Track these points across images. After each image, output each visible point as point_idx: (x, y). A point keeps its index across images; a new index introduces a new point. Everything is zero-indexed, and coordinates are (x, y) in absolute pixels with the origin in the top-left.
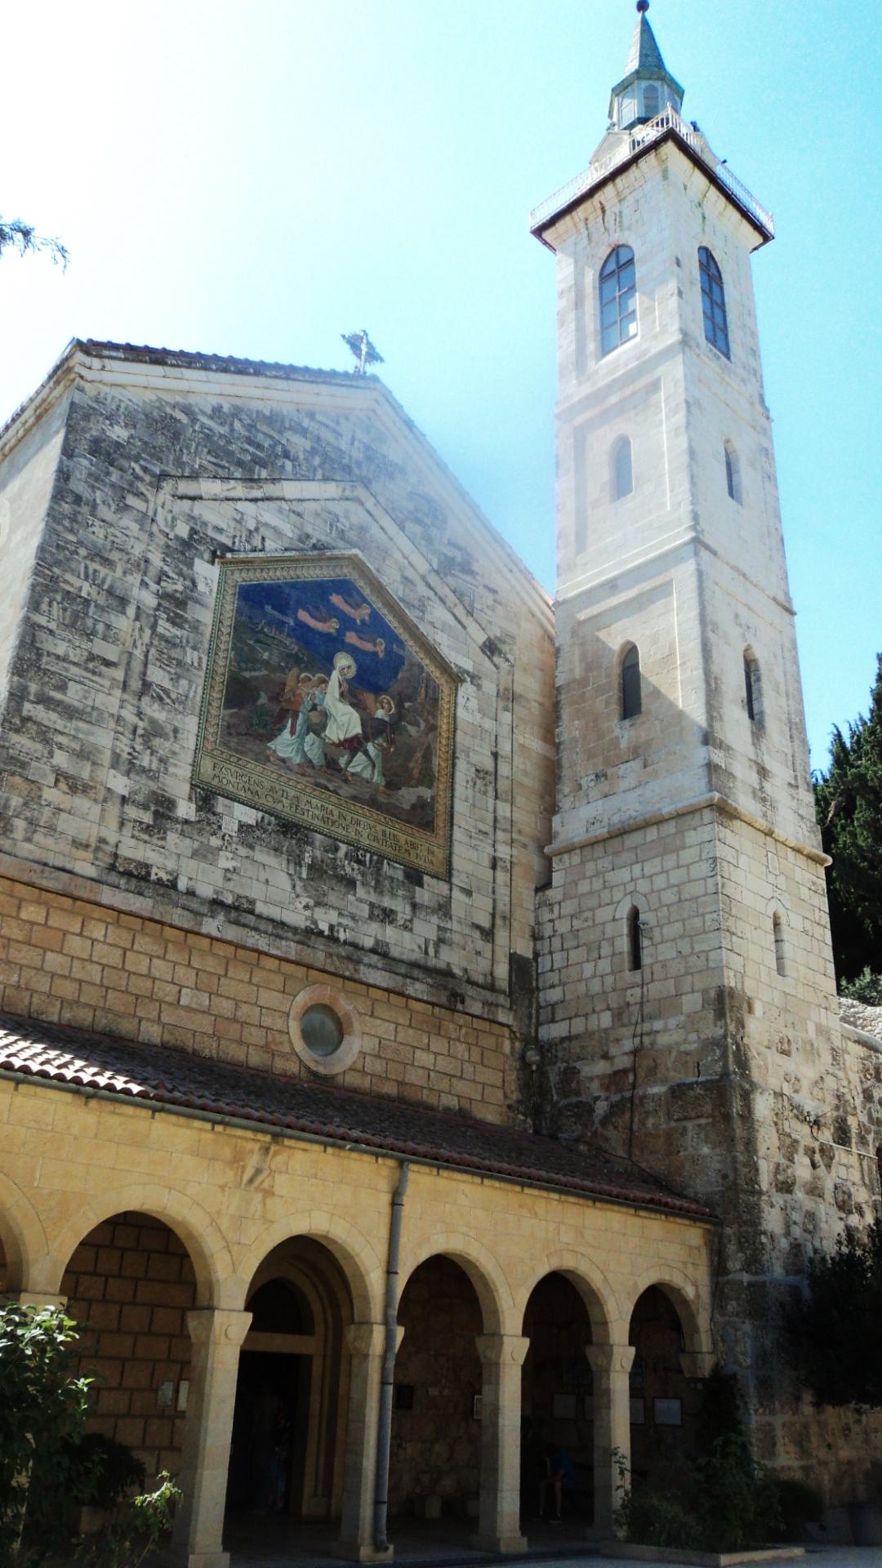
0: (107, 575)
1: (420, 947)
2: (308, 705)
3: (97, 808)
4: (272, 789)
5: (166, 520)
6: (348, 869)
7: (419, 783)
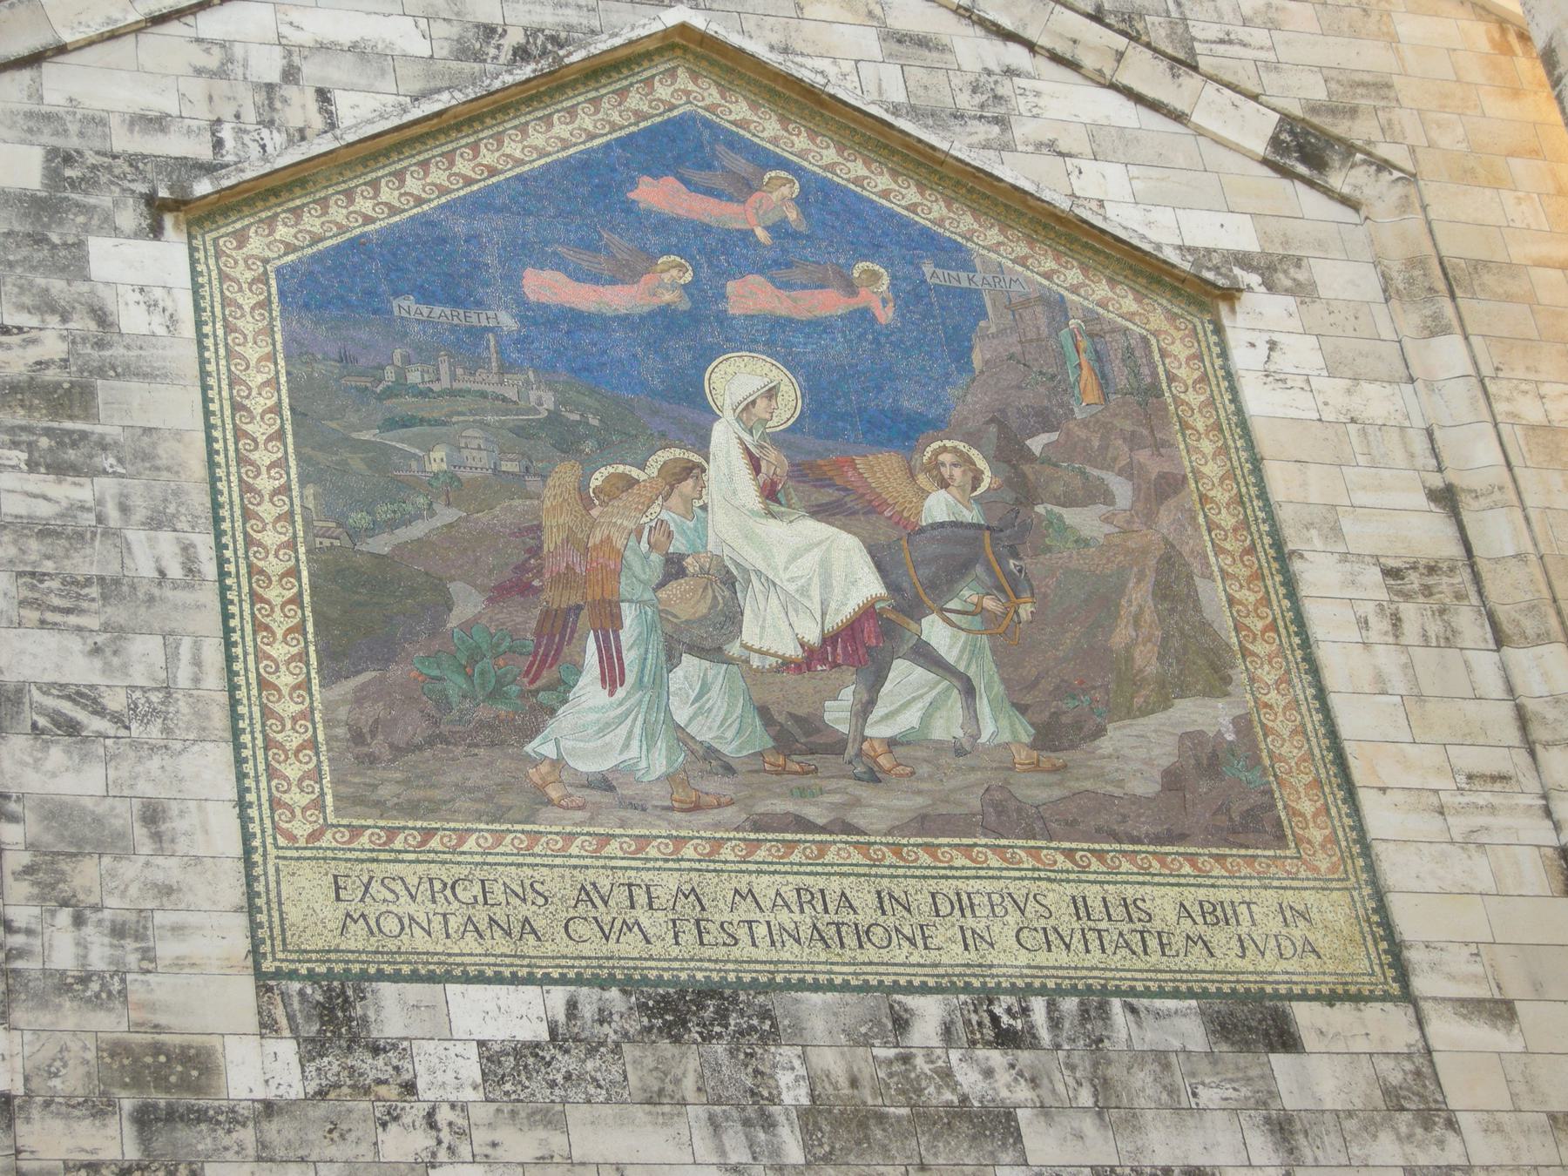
2: (642, 565)
4: (585, 894)
6: (969, 1079)
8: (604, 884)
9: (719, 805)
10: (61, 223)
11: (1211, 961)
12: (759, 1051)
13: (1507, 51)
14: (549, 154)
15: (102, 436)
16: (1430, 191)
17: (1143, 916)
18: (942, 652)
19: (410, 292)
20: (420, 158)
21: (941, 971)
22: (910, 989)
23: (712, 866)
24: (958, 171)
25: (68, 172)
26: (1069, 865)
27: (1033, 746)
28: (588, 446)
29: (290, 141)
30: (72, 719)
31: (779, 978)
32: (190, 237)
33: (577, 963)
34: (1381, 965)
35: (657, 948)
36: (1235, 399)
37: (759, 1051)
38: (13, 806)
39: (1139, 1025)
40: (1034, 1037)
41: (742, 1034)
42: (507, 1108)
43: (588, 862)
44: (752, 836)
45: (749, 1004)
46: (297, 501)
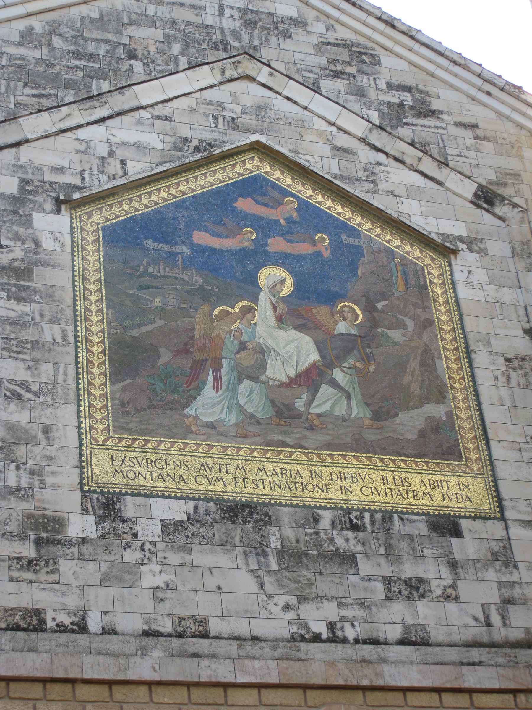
1: (476, 619)
6: (340, 542)
8: (210, 463)
9: (254, 436)
10: (24, 207)
11: (432, 502)
12: (264, 528)
14: (205, 188)
15: (35, 288)
17: (408, 484)
18: (340, 382)
21: (332, 501)
23: (250, 459)
25: (27, 188)
26: (382, 464)
27: (371, 419)
28: (214, 299)
29: (110, 180)
30: (19, 393)
31: (272, 501)
32: (71, 214)
33: (198, 492)
34: (494, 506)
35: (228, 489)
36: (455, 292)
37: (264, 528)
39: (403, 524)
40: (365, 527)
41: (258, 521)
42: (170, 545)
43: (205, 455)
44: (266, 448)
45: (261, 510)
46: (105, 315)
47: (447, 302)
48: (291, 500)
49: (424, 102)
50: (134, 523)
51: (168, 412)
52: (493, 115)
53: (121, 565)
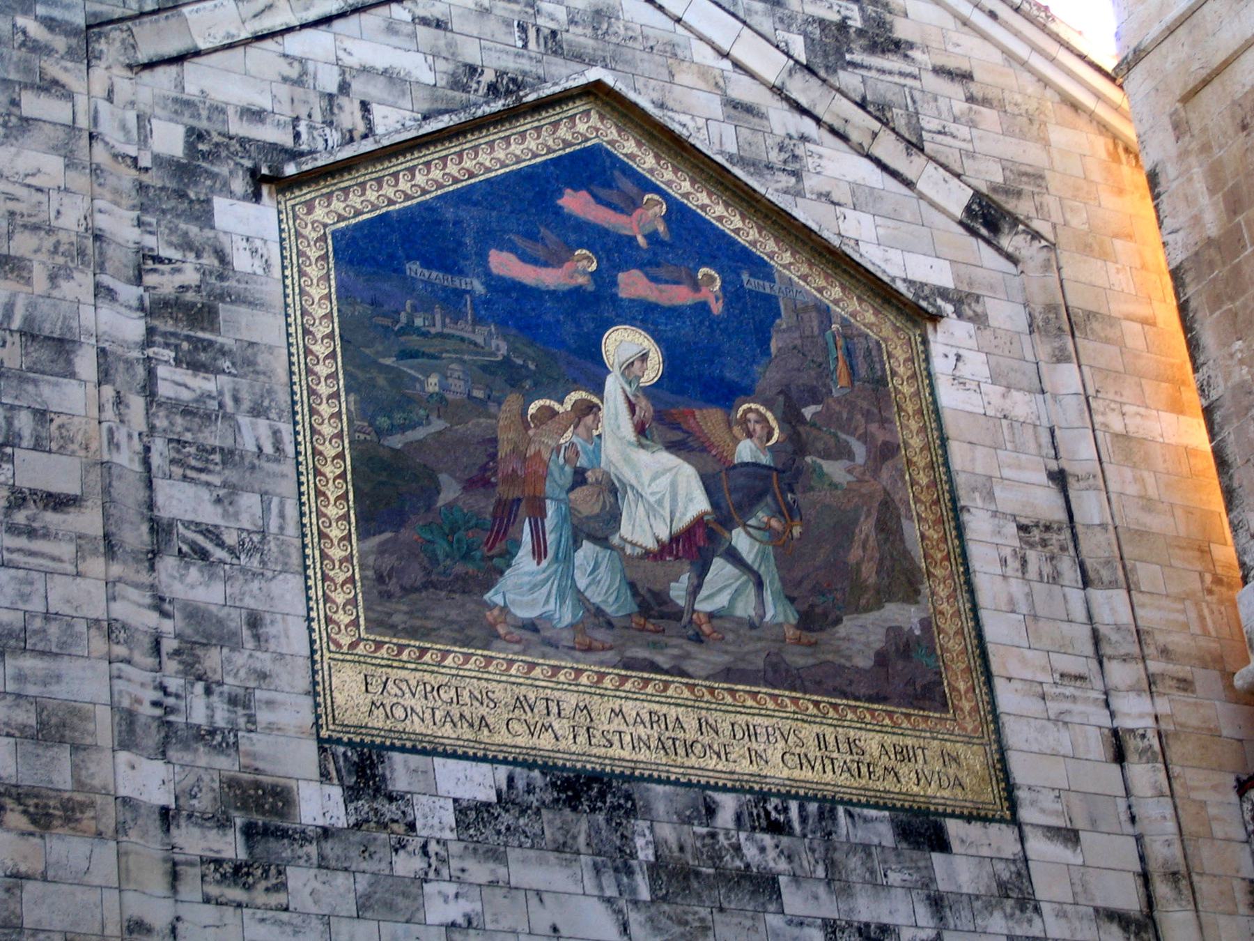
0: (14, 295)
2: (560, 475)
3: (108, 851)
4: (519, 702)
5: (124, 127)
6: (750, 852)
7: (882, 596)
8: (532, 696)
9: (603, 649)
10: (196, 183)
13: (1117, 160)
14: (507, 166)
15: (222, 346)
16: (1064, 257)
18: (744, 555)
19: (417, 259)
20: (425, 159)
21: (736, 777)
22: (716, 788)
24: (768, 208)
25: (201, 147)
26: (815, 712)
27: (797, 627)
28: (528, 384)
31: (637, 773)
35: (562, 745)
36: (932, 393)
37: (625, 822)
38: (167, 607)
39: (854, 825)
42: (471, 846)
43: (521, 680)
44: (623, 672)
45: (619, 789)
46: (344, 405)
47: (920, 412)
48: (668, 771)
49: (881, 24)
50: (409, 803)
51: (457, 596)
52: (997, 57)
53: (390, 880)
